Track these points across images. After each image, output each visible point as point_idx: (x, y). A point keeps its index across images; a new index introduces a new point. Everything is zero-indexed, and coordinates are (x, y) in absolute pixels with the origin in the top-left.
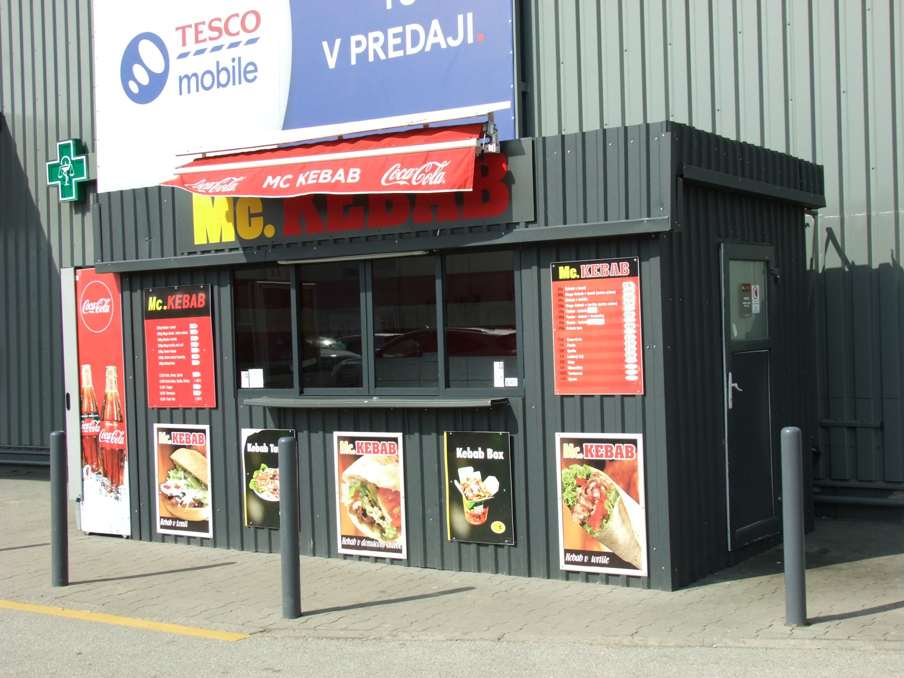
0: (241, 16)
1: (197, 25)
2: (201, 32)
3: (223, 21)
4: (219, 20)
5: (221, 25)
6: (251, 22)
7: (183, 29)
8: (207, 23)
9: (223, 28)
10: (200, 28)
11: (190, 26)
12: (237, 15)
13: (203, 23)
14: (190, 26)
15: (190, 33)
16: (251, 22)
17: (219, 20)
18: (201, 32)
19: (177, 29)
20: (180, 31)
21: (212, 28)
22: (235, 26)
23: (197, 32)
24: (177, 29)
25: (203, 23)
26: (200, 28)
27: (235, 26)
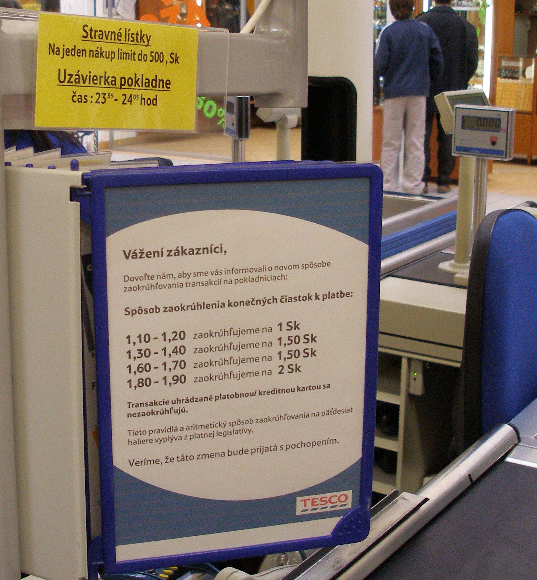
0: (338, 496)
1: (313, 499)
2: (316, 502)
3: (328, 498)
4: (327, 497)
5: (327, 499)
10: (315, 500)
11: (309, 500)
12: (336, 496)
13: (318, 499)
14: (309, 500)
15: (309, 503)
17: (327, 497)
18: (316, 502)
19: (301, 501)
20: (303, 502)
21: (321, 500)
23: (313, 502)
24: (301, 501)
25: (318, 499)
26: (315, 500)
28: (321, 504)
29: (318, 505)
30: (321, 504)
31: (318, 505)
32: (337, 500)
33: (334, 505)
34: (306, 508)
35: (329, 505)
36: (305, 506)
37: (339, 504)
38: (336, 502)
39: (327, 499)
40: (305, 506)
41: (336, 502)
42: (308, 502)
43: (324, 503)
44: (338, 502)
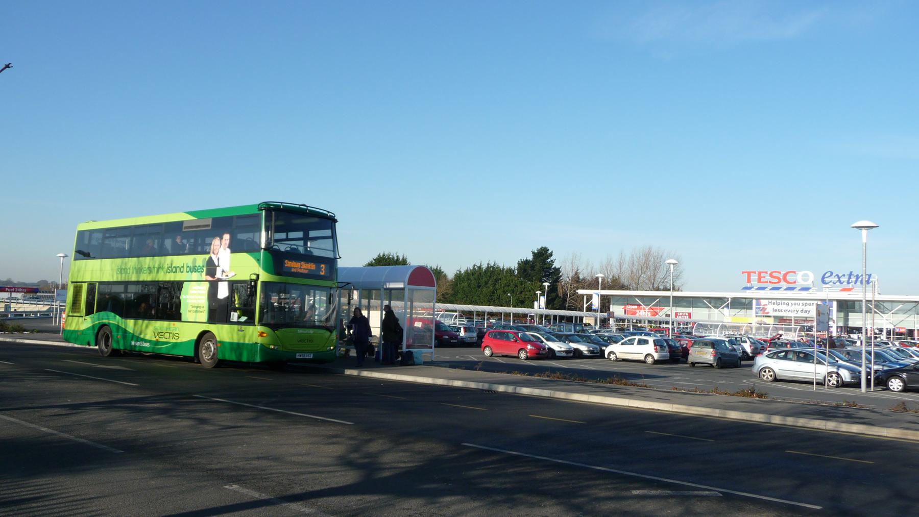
1: (760, 273)
2: (764, 277)
4: (780, 273)
7: (749, 274)
8: (769, 272)
9: (782, 278)
10: (763, 275)
11: (755, 273)
13: (767, 273)
14: (755, 273)
15: (754, 277)
18: (764, 277)
19: (743, 272)
20: (746, 274)
21: (771, 275)
24: (743, 272)
25: (767, 273)
26: (763, 275)
28: (771, 282)
29: (767, 282)
30: (771, 282)
31: (767, 282)
33: (791, 286)
34: (749, 285)
35: (783, 284)
36: (749, 281)
40: (749, 281)
42: (752, 274)
43: (777, 280)
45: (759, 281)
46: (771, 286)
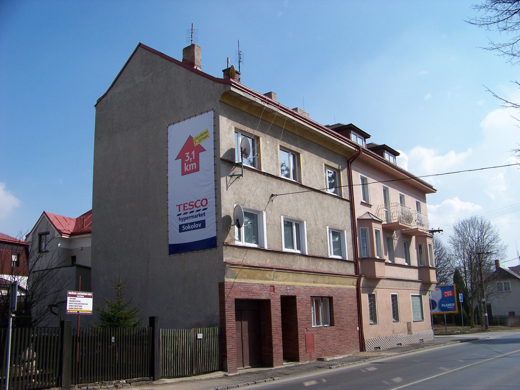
1: (184, 204)
2: (186, 207)
3: (194, 203)
4: (193, 202)
5: (193, 204)
6: (204, 202)
7: (179, 206)
10: (185, 205)
11: (182, 205)
12: (199, 200)
13: (187, 203)
14: (182, 205)
15: (182, 207)
16: (204, 202)
17: (193, 202)
18: (186, 207)
19: (177, 206)
20: (178, 206)
21: (190, 205)
22: (198, 204)
23: (184, 207)
24: (177, 206)
25: (187, 203)
26: (185, 205)
27: (198, 204)
28: (189, 209)
29: (187, 209)
30: (189, 209)
31: (187, 209)
32: (200, 204)
35: (195, 209)
36: (179, 211)
37: (202, 208)
38: (200, 206)
39: (193, 204)
40: (179, 211)
41: (200, 206)
42: (181, 206)
43: (192, 207)
44: (201, 206)
45: (184, 210)
46: (189, 211)
